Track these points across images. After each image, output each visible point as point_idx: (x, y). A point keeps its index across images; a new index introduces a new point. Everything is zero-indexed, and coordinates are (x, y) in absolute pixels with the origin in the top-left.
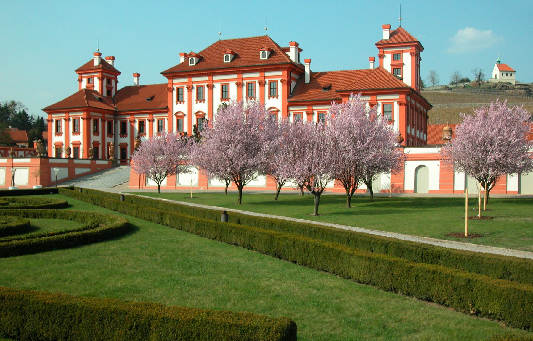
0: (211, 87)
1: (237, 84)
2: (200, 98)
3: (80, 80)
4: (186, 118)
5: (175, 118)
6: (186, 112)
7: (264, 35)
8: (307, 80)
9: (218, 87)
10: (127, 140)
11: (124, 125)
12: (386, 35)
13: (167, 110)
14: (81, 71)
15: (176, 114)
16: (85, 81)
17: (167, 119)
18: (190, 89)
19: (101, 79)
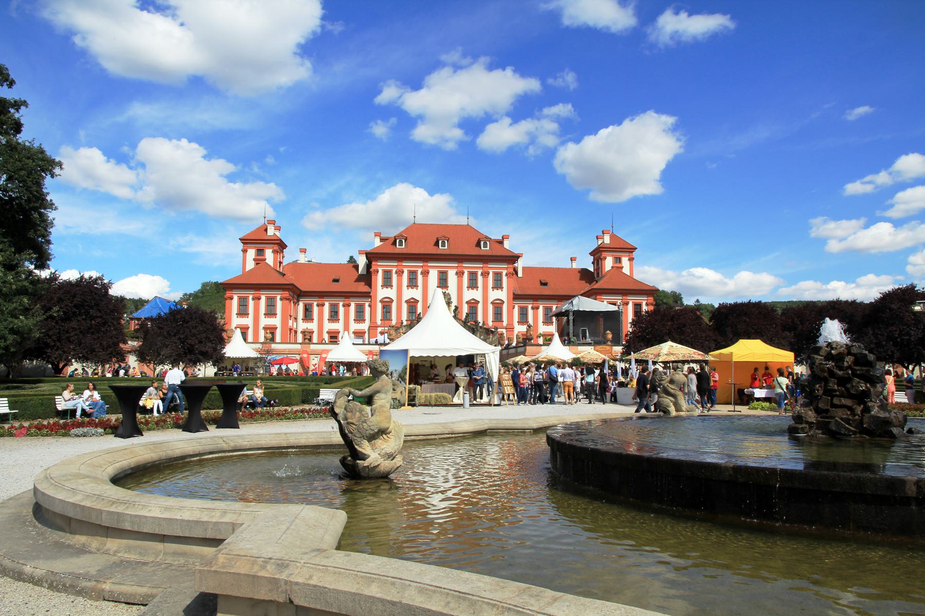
0: (425, 274)
1: (457, 273)
2: (412, 284)
3: (245, 251)
4: (394, 305)
5: (379, 306)
6: (394, 297)
8: (520, 274)
9: (433, 275)
10: (313, 326)
11: (308, 310)
12: (607, 239)
15: (381, 301)
16: (251, 253)
17: (370, 306)
18: (400, 273)
19: (274, 252)
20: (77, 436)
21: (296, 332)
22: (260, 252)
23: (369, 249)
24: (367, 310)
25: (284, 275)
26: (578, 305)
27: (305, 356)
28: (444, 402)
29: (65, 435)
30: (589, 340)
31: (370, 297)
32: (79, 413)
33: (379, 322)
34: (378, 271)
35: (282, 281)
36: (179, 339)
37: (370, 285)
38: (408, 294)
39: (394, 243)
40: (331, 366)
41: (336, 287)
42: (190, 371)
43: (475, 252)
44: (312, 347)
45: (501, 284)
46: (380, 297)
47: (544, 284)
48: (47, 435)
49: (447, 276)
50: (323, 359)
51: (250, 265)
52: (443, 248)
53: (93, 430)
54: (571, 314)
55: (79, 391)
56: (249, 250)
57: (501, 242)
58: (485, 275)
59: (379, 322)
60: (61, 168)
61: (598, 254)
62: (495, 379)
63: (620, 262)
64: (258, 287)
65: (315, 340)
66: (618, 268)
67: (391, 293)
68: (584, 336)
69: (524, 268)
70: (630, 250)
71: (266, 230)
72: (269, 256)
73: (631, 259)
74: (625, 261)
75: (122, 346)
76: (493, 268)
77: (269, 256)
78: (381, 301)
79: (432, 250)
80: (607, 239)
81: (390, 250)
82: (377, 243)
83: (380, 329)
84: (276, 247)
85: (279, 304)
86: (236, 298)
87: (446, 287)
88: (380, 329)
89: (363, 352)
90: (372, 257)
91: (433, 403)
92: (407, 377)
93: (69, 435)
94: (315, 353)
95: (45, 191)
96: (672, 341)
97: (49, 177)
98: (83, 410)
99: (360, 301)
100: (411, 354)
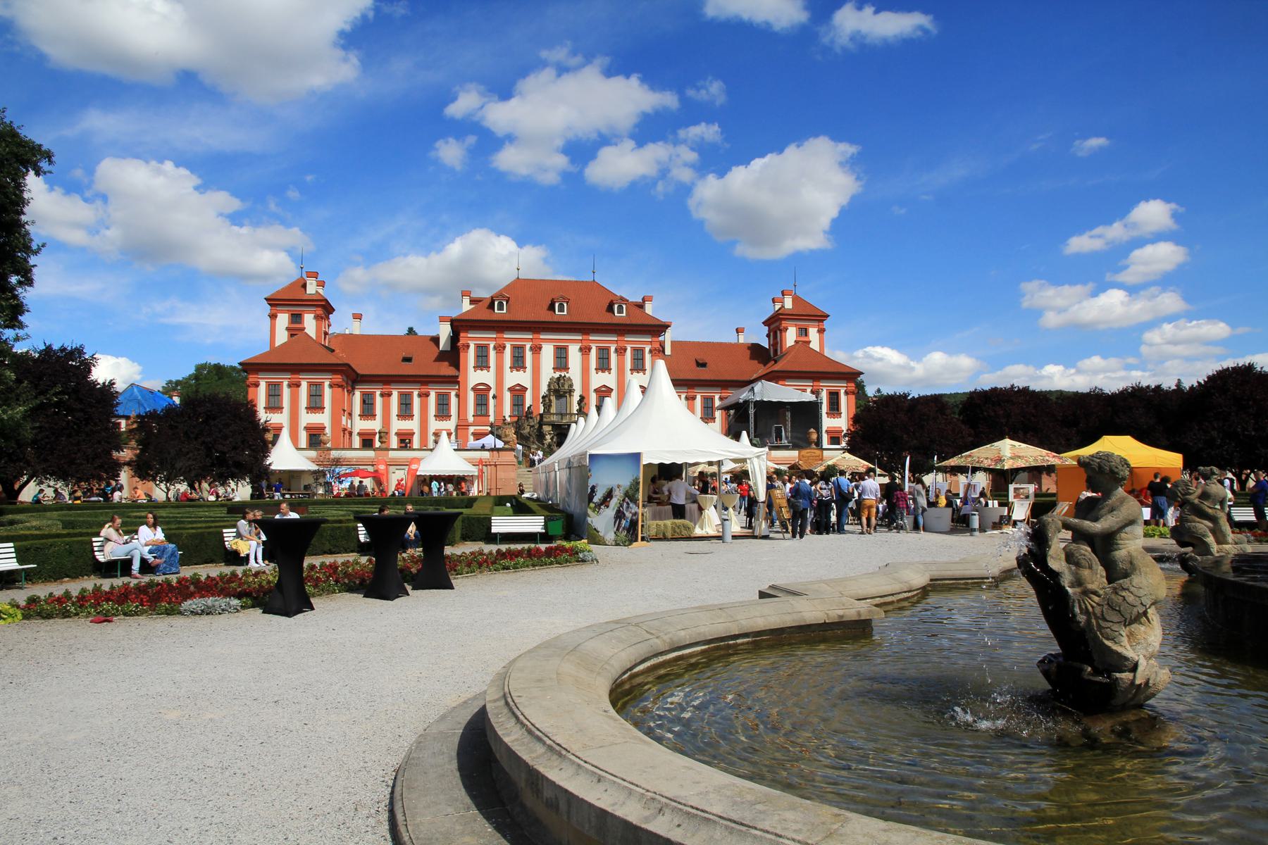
0: (537, 350)
1: (581, 349)
2: (518, 364)
3: (273, 317)
5: (471, 396)
6: (492, 385)
7: (588, 278)
8: (668, 351)
9: (548, 351)
12: (788, 303)
13: (453, 380)
14: (275, 303)
15: (474, 389)
16: (283, 319)
17: (458, 396)
18: (500, 349)
19: (317, 318)
20: (194, 613)
21: (351, 434)
22: (296, 318)
23: (454, 315)
24: (454, 401)
25: (333, 351)
26: (762, 393)
27: (382, 467)
28: (685, 533)
29: (169, 613)
30: (785, 442)
31: (458, 383)
32: (136, 566)
33: (471, 419)
34: (468, 346)
35: (331, 359)
36: (204, 442)
37: (457, 367)
38: (513, 378)
39: (491, 306)
40: (426, 480)
41: (407, 369)
42: (221, 491)
43: (605, 318)
44: (392, 454)
45: (643, 364)
46: (471, 384)
47: (704, 365)
48: (136, 614)
49: (567, 352)
50: (412, 473)
51: (282, 337)
52: (561, 314)
53: (221, 602)
54: (752, 406)
55: (130, 529)
56: (279, 315)
57: (641, 306)
58: (621, 351)
59: (471, 419)
60: (51, 162)
61: (775, 324)
62: (762, 497)
63: (806, 335)
64: (296, 369)
65: (416, 444)
66: (803, 344)
67: (487, 377)
68: (779, 437)
69: (673, 343)
70: (820, 318)
71: (304, 286)
72: (310, 323)
73: (821, 331)
74: (813, 333)
75: (115, 454)
76: (631, 342)
77: (310, 323)
78: (474, 389)
79: (545, 316)
80: (788, 303)
81: (485, 315)
82: (466, 306)
83: (472, 429)
84: (320, 311)
85: (327, 392)
86: (263, 384)
87: (566, 369)
88: (472, 429)
89: (470, 461)
90: (459, 326)
91: (669, 535)
92: (640, 496)
93: (180, 613)
94: (398, 464)
95: (26, 195)
96: (1011, 438)
97: (32, 173)
98: (143, 561)
99: (443, 389)
100: (645, 461)
